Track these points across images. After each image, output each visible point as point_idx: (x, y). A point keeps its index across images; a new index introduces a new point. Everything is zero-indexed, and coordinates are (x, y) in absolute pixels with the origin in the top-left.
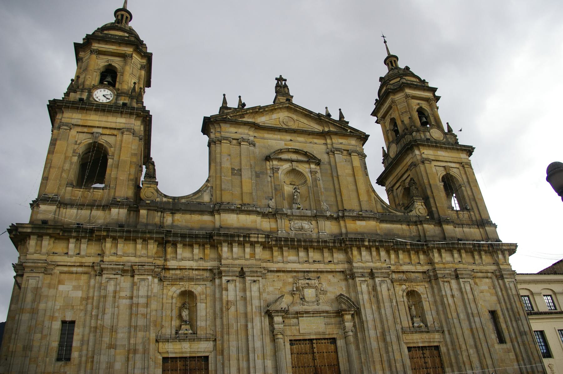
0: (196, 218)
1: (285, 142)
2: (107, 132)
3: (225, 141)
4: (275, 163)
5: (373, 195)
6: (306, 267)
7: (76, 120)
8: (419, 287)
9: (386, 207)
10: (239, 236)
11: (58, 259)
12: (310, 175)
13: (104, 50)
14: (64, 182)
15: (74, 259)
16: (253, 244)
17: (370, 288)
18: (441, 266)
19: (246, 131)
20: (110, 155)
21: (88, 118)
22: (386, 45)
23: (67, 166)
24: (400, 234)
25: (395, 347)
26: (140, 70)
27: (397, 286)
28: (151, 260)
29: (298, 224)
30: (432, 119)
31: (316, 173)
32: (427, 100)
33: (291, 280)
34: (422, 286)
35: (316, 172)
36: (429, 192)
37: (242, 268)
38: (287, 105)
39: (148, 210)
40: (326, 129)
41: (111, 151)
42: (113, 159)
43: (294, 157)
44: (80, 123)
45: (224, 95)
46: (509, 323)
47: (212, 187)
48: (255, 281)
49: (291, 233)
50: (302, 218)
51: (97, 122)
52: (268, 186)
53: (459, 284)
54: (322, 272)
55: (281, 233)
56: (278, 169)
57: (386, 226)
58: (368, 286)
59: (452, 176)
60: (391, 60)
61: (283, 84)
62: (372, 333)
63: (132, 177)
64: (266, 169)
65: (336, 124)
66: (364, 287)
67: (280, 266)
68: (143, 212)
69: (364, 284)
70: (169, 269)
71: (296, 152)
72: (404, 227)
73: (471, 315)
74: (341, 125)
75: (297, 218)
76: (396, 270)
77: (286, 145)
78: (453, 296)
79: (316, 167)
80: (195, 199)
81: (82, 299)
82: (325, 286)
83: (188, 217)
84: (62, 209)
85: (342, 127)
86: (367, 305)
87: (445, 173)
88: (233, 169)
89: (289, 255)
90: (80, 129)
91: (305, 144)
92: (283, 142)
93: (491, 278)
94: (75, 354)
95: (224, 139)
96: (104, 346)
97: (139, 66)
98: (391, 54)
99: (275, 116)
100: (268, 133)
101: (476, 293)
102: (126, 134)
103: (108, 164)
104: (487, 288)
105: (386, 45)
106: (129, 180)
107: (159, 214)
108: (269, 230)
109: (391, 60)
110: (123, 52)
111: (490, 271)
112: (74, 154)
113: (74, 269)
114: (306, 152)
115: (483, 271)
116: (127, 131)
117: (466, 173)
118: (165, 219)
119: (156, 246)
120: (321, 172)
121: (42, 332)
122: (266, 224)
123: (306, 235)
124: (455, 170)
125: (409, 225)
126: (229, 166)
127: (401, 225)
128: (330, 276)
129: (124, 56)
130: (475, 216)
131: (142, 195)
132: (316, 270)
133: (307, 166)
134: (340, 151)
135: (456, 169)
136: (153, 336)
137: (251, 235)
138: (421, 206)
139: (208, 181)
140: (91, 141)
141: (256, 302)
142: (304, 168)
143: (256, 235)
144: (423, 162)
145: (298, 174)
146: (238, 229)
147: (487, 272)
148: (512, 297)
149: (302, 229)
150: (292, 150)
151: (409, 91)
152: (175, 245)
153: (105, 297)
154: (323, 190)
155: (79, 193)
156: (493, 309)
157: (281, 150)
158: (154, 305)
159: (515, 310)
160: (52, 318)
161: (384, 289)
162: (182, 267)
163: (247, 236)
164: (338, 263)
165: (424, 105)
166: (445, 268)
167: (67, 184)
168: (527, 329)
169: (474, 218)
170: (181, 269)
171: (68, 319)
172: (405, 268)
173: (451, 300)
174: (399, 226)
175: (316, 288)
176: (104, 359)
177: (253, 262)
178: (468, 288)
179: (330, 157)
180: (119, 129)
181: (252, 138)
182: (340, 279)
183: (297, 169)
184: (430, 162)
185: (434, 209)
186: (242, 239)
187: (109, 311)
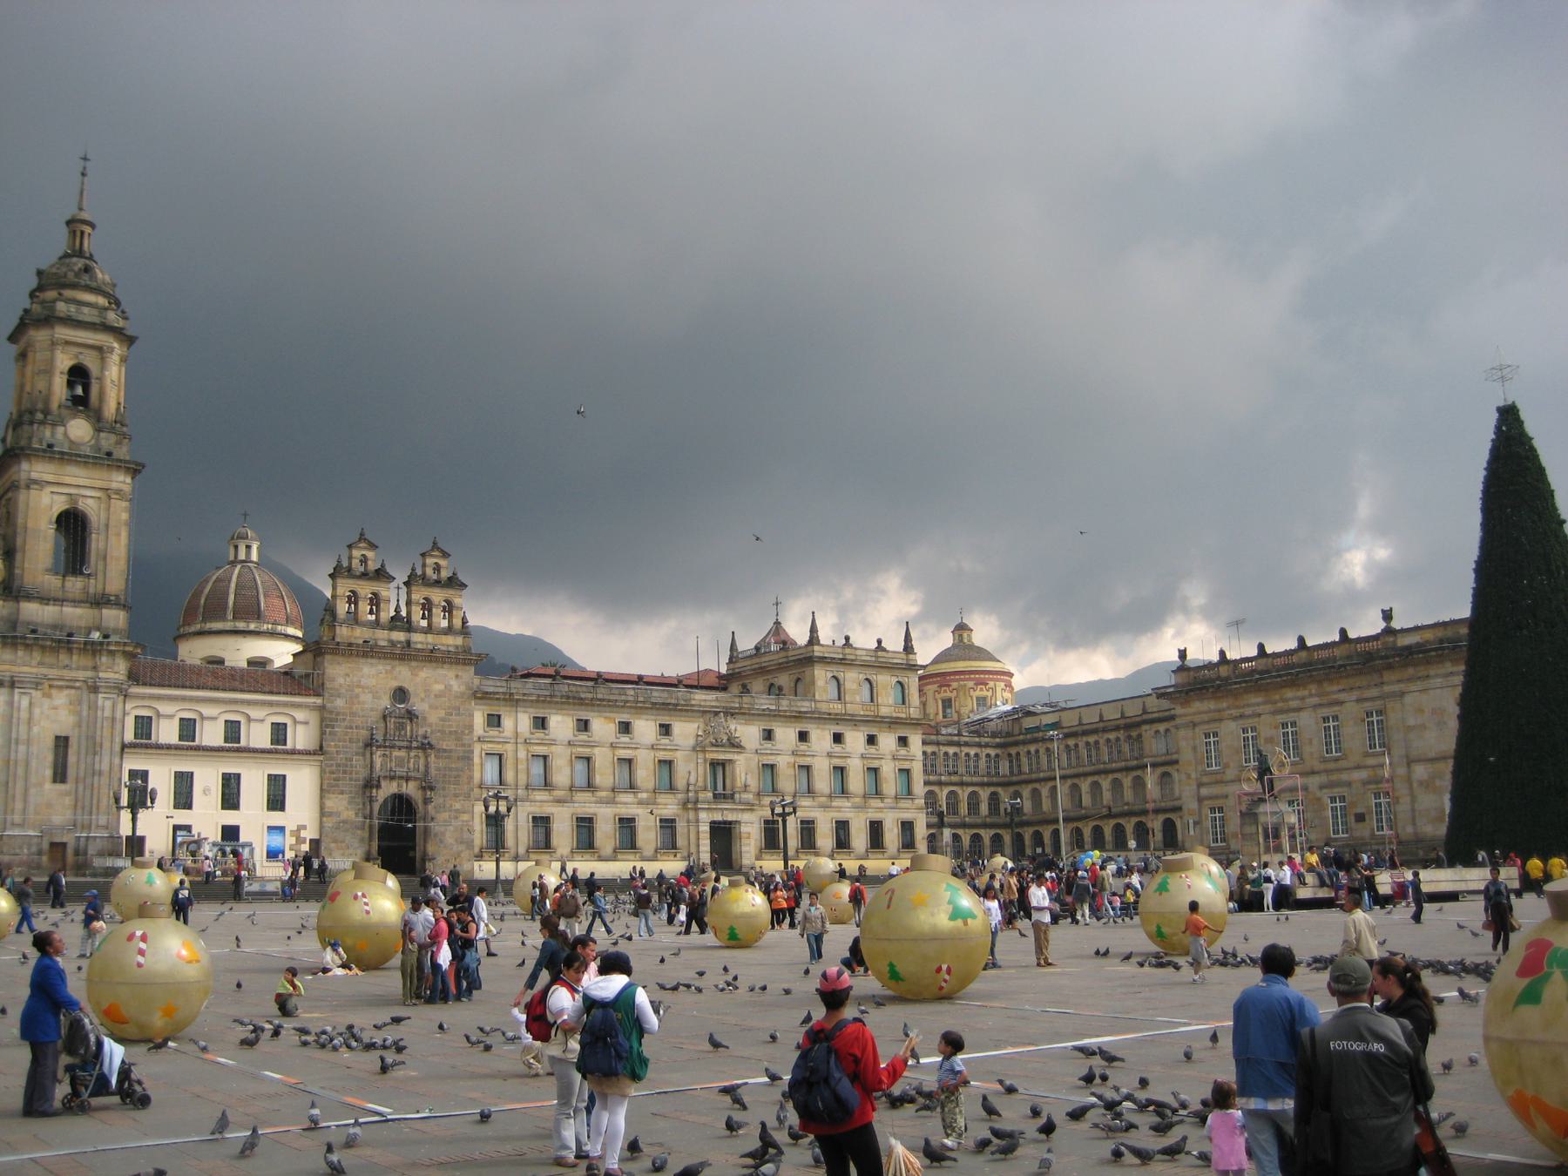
32: (99, 349)
36: (19, 541)
46: (83, 756)
59: (82, 511)
73: (13, 741)
87: (67, 507)
101: (37, 711)
117: (108, 509)
124: (90, 501)
130: (94, 586)
144: (28, 487)
148: (99, 721)
156: (63, 735)
159: (98, 740)
168: (105, 767)
169: (92, 590)
178: (25, 702)
185: (17, 571)
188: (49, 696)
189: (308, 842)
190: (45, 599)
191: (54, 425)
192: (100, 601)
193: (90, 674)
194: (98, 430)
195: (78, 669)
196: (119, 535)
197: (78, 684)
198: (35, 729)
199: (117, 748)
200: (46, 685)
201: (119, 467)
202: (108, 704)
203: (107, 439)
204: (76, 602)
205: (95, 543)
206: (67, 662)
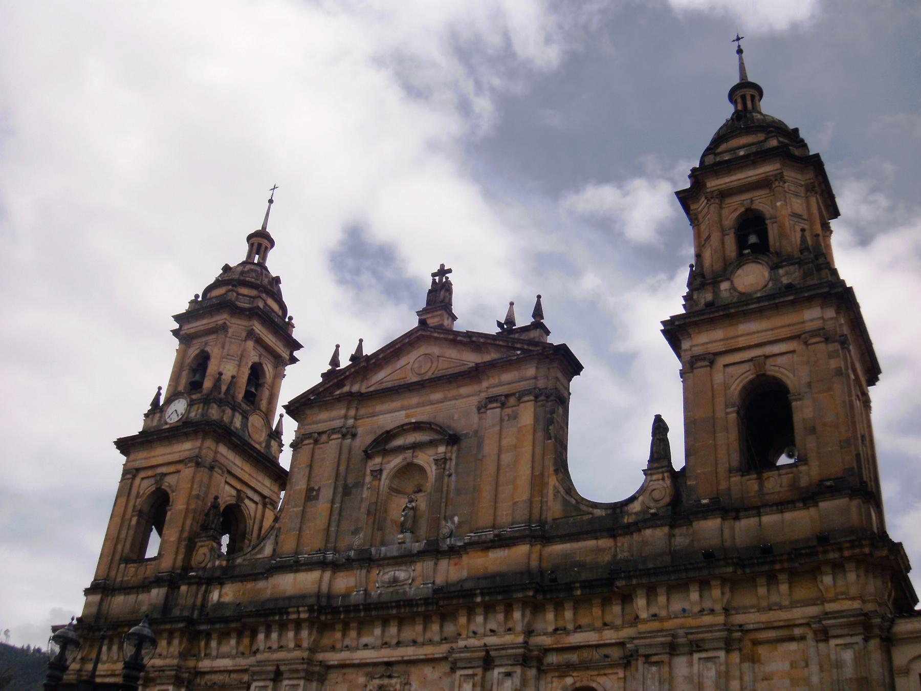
0: (249, 586)
1: (408, 411)
2: (171, 469)
3: (307, 442)
4: (378, 460)
5: (553, 481)
7: (140, 461)
8: (601, 680)
9: (574, 502)
10: (274, 614)
12: (434, 467)
13: (193, 331)
14: (117, 557)
16: (298, 625)
18: (655, 625)
19: (343, 412)
20: (170, 504)
21: (152, 454)
22: (741, 59)
23: (123, 535)
24: (588, 561)
26: (246, 340)
27: (555, 680)
28: (175, 662)
29: (389, 574)
30: (773, 232)
31: (445, 463)
32: (764, 184)
33: (362, 680)
34: (611, 676)
35: (445, 460)
37: (278, 666)
38: (420, 333)
39: (190, 584)
40: (487, 358)
41: (172, 496)
42: (170, 510)
43: (412, 438)
44: (145, 464)
45: (338, 346)
47: (280, 528)
48: (294, 685)
49: (373, 593)
50: (399, 560)
51: (160, 458)
52: (359, 509)
53: (691, 664)
55: (356, 595)
56: (381, 471)
57: (558, 548)
58: (474, 686)
61: (444, 280)
63: (185, 535)
64: (364, 475)
65: (497, 342)
67: (344, 656)
68: (184, 588)
69: (468, 683)
71: (417, 427)
72: (605, 543)
74: (507, 342)
75: (390, 561)
76: (554, 646)
79: (449, 448)
80: (253, 555)
84: (109, 598)
85: (510, 344)
87: (751, 377)
88: (310, 490)
89: (359, 635)
90: (143, 474)
91: (442, 404)
92: (403, 413)
93: (803, 638)
95: (306, 439)
97: (244, 334)
98: (751, 79)
99: (402, 362)
100: (383, 403)
102: (188, 467)
103: (167, 519)
104: (786, 666)
105: (741, 59)
106: (179, 540)
107: (204, 587)
108: (343, 591)
110: (213, 325)
111: (797, 622)
112: (134, 513)
114: (430, 424)
115: (776, 624)
116: (189, 461)
118: (211, 595)
119: (185, 640)
120: (457, 458)
122: (344, 582)
123: (397, 593)
124: (780, 360)
125: (614, 537)
127: (597, 538)
128: (427, 670)
129: (214, 331)
131: (194, 563)
132: (400, 659)
133: (431, 451)
134: (497, 401)
135: (790, 356)
137: (290, 610)
138: (661, 482)
140: (154, 489)
142: (425, 459)
143: (295, 609)
145: (421, 470)
146: (290, 598)
147: (790, 625)
149: (395, 580)
150: (409, 426)
151: (713, 184)
152: (208, 636)
154: (452, 495)
155: (132, 568)
157: (388, 432)
162: (215, 669)
163: (283, 611)
165: (761, 201)
166: (662, 630)
167: (121, 559)
170: (216, 672)
172: (577, 638)
174: (591, 543)
177: (298, 654)
178: (710, 673)
179: (480, 419)
181: (351, 422)
182: (445, 673)
183: (416, 461)
184: (712, 363)
186: (277, 618)
188: (754, 659)
191: (715, 282)
193: (813, 610)
194: (774, 267)
195: (793, 605)
196: (830, 389)
197: (797, 632)
200: (747, 644)
201: (810, 299)
202: (848, 656)
203: (787, 274)
204: (782, 505)
206: (774, 598)
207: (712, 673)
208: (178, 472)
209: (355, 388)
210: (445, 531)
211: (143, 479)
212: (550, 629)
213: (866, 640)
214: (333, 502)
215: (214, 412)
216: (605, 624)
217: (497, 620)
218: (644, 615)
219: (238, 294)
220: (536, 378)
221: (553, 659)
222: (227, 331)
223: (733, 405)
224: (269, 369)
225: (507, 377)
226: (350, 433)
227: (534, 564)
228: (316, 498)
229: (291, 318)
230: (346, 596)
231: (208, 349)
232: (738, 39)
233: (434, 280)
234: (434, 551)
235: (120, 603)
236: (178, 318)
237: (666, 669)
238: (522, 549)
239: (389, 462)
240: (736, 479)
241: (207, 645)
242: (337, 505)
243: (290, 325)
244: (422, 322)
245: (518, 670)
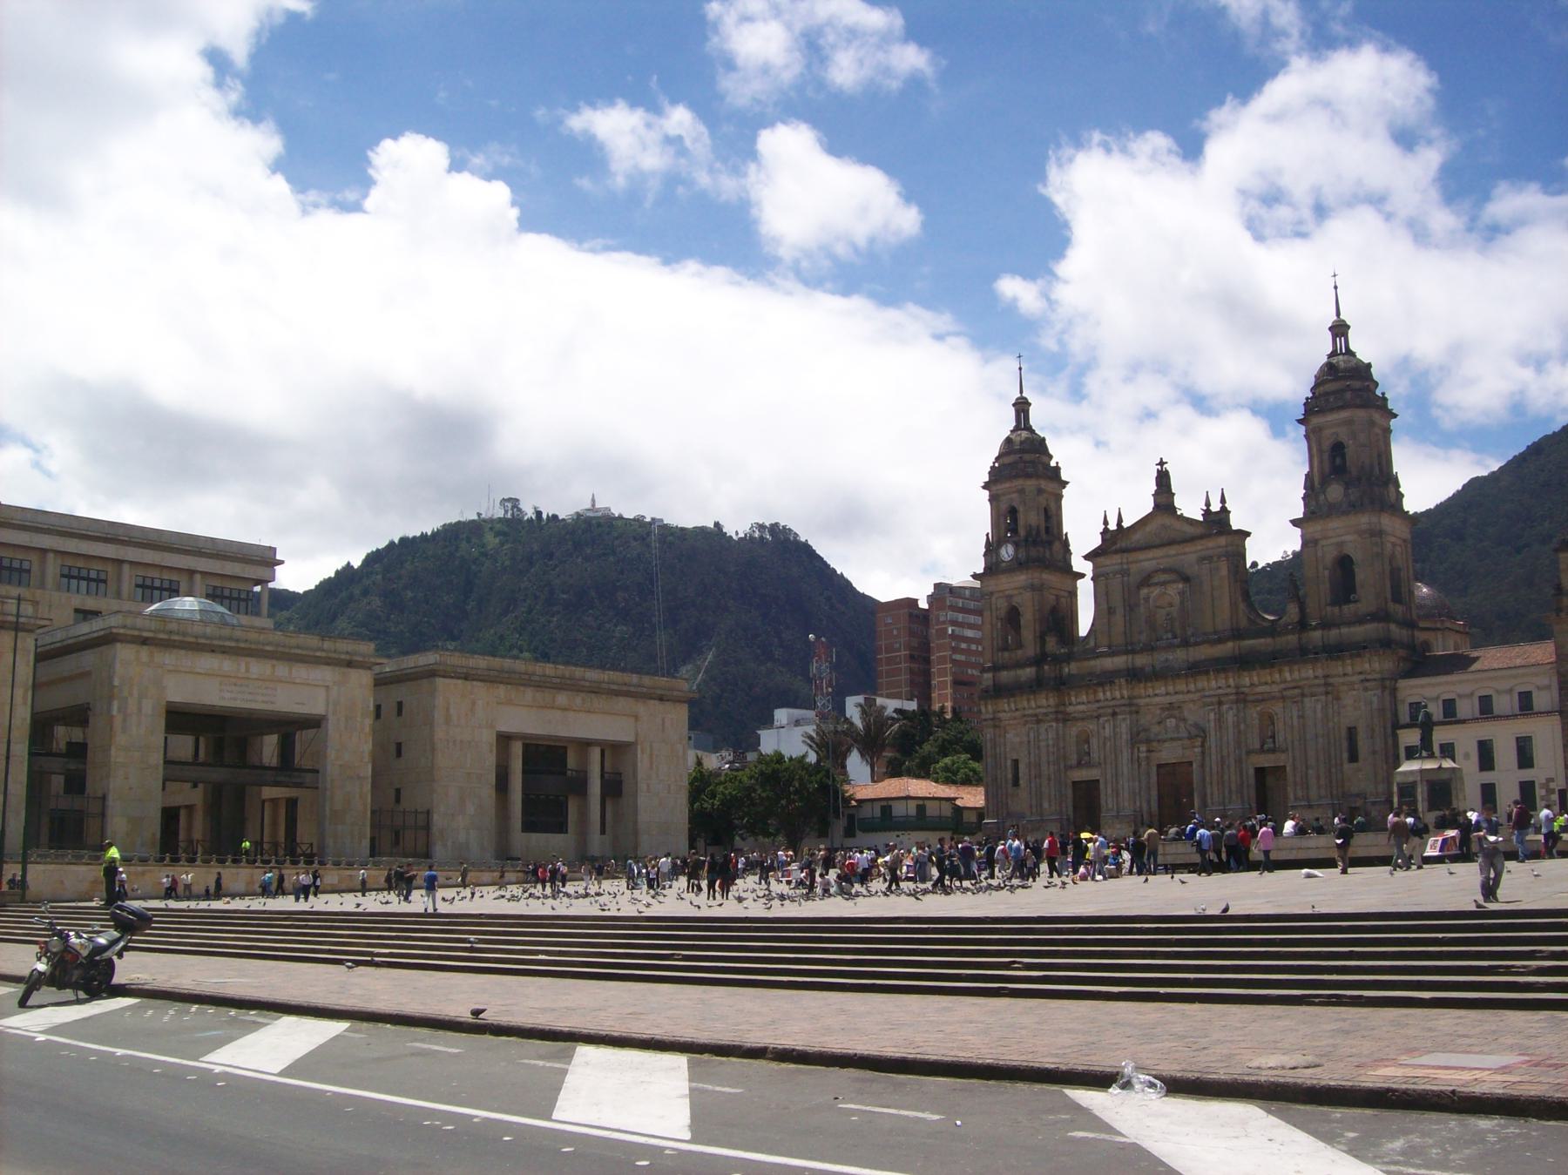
2: (1016, 592)
5: (1242, 606)
6: (1168, 699)
11: (1001, 715)
15: (1009, 714)
17: (1217, 715)
18: (1293, 684)
23: (995, 636)
25: (1232, 769)
33: (1158, 712)
54: (1184, 702)
57: (1248, 643)
58: (1215, 714)
60: (1340, 329)
62: (1214, 757)
63: (1038, 634)
66: (1212, 716)
70: (1071, 714)
71: (1164, 571)
72: (1269, 640)
77: (1158, 564)
78: (1299, 717)
81: (1021, 743)
82: (1186, 714)
83: (1079, 664)
86: (1213, 733)
87: (1336, 553)
88: (1109, 609)
90: (996, 595)
92: (1154, 562)
94: (1021, 782)
96: (1033, 776)
99: (1148, 529)
109: (1340, 329)
113: (1011, 722)
121: (1001, 768)
122: (1141, 660)
125: (1273, 637)
126: (1105, 607)
128: (1191, 705)
133: (1175, 586)
136: (1062, 766)
139: (1093, 625)
141: (1124, 737)
147: (1352, 683)
149: (1167, 660)
153: (1029, 742)
155: (1006, 654)
158: (1061, 745)
160: (1006, 759)
161: (1230, 717)
164: (1195, 692)
171: (1014, 758)
173: (1295, 723)
174: (1262, 640)
175: (1175, 717)
176: (1033, 785)
177: (1123, 702)
180: (1021, 588)
181: (1125, 567)
187: (1032, 751)
189: (1557, 793)
190: (1325, 625)
192: (1361, 620)
193: (1362, 677)
194: (1347, 488)
197: (1356, 686)
198: (1331, 724)
199: (1389, 731)
202: (1375, 699)
204: (1349, 624)
205: (1361, 575)
207: (1319, 707)
208: (1021, 594)
209: (1124, 545)
210: (1189, 633)
211: (997, 599)
212: (1248, 684)
213: (1383, 692)
214: (1125, 616)
215: (1033, 553)
216: (1273, 682)
217: (1222, 682)
218: (1289, 679)
219: (1025, 462)
220: (1226, 546)
221: (1250, 698)
222: (1025, 493)
223: (1327, 569)
224: (1053, 505)
225: (1210, 543)
226: (1125, 573)
227: (1237, 652)
228: (1114, 612)
229: (1057, 463)
230: (1142, 669)
231: (1015, 504)
232: (1335, 276)
233: (1158, 470)
234: (1186, 643)
235: (1005, 676)
236: (985, 483)
237: (1300, 704)
238: (1230, 644)
239: (1152, 592)
240: (1329, 609)
241: (1070, 699)
242: (1127, 618)
243: (1057, 469)
244: (1157, 506)
245: (1234, 706)
